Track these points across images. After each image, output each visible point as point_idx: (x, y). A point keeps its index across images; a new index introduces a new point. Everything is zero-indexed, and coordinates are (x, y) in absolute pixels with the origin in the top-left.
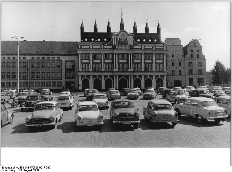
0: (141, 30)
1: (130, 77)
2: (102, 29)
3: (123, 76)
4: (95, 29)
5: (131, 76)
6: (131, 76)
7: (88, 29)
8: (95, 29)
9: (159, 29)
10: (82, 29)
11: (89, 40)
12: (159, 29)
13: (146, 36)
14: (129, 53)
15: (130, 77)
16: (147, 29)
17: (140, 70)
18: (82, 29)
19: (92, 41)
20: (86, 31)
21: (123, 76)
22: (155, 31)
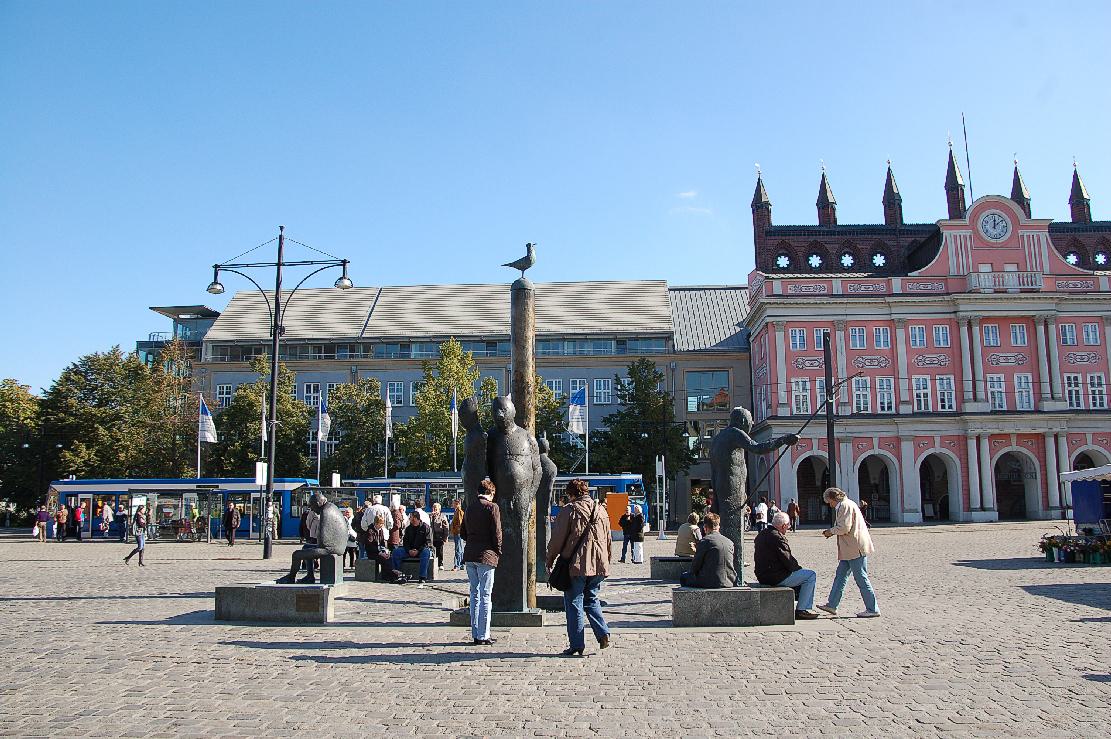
1: (1051, 442)
2: (860, 209)
3: (1014, 440)
4: (825, 206)
6: (1056, 437)
7: (795, 211)
8: (825, 206)
10: (760, 208)
11: (798, 266)
13: (1082, 237)
15: (1051, 442)
16: (1078, 201)
17: (1098, 407)
18: (760, 208)
19: (812, 270)
20: (777, 220)
21: (1014, 440)
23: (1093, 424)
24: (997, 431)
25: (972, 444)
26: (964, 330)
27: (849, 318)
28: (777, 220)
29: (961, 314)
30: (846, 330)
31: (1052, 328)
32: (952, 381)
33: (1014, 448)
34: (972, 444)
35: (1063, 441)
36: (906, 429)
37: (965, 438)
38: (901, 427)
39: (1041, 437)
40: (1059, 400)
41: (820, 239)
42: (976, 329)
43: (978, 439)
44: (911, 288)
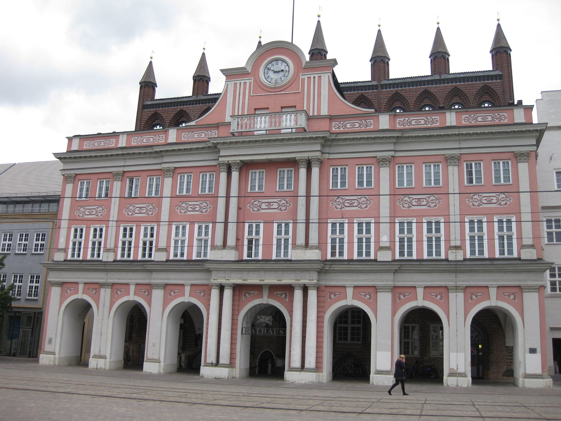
0: (410, 63)
1: (298, 294)
5: (305, 289)
6: (305, 289)
9: (501, 52)
10: (148, 85)
12: (501, 52)
14: (298, 156)
15: (298, 294)
20: (160, 94)
22: (484, 63)
23: (355, 277)
24: (240, 281)
26: (223, 176)
27: (126, 169)
28: (160, 94)
29: (221, 159)
31: (315, 171)
33: (265, 300)
34: (215, 293)
35: (313, 295)
36: (159, 278)
37: (208, 288)
38: (155, 275)
39: (290, 288)
40: (313, 248)
41: (185, 108)
42: (235, 175)
43: (222, 288)
44: (186, 137)
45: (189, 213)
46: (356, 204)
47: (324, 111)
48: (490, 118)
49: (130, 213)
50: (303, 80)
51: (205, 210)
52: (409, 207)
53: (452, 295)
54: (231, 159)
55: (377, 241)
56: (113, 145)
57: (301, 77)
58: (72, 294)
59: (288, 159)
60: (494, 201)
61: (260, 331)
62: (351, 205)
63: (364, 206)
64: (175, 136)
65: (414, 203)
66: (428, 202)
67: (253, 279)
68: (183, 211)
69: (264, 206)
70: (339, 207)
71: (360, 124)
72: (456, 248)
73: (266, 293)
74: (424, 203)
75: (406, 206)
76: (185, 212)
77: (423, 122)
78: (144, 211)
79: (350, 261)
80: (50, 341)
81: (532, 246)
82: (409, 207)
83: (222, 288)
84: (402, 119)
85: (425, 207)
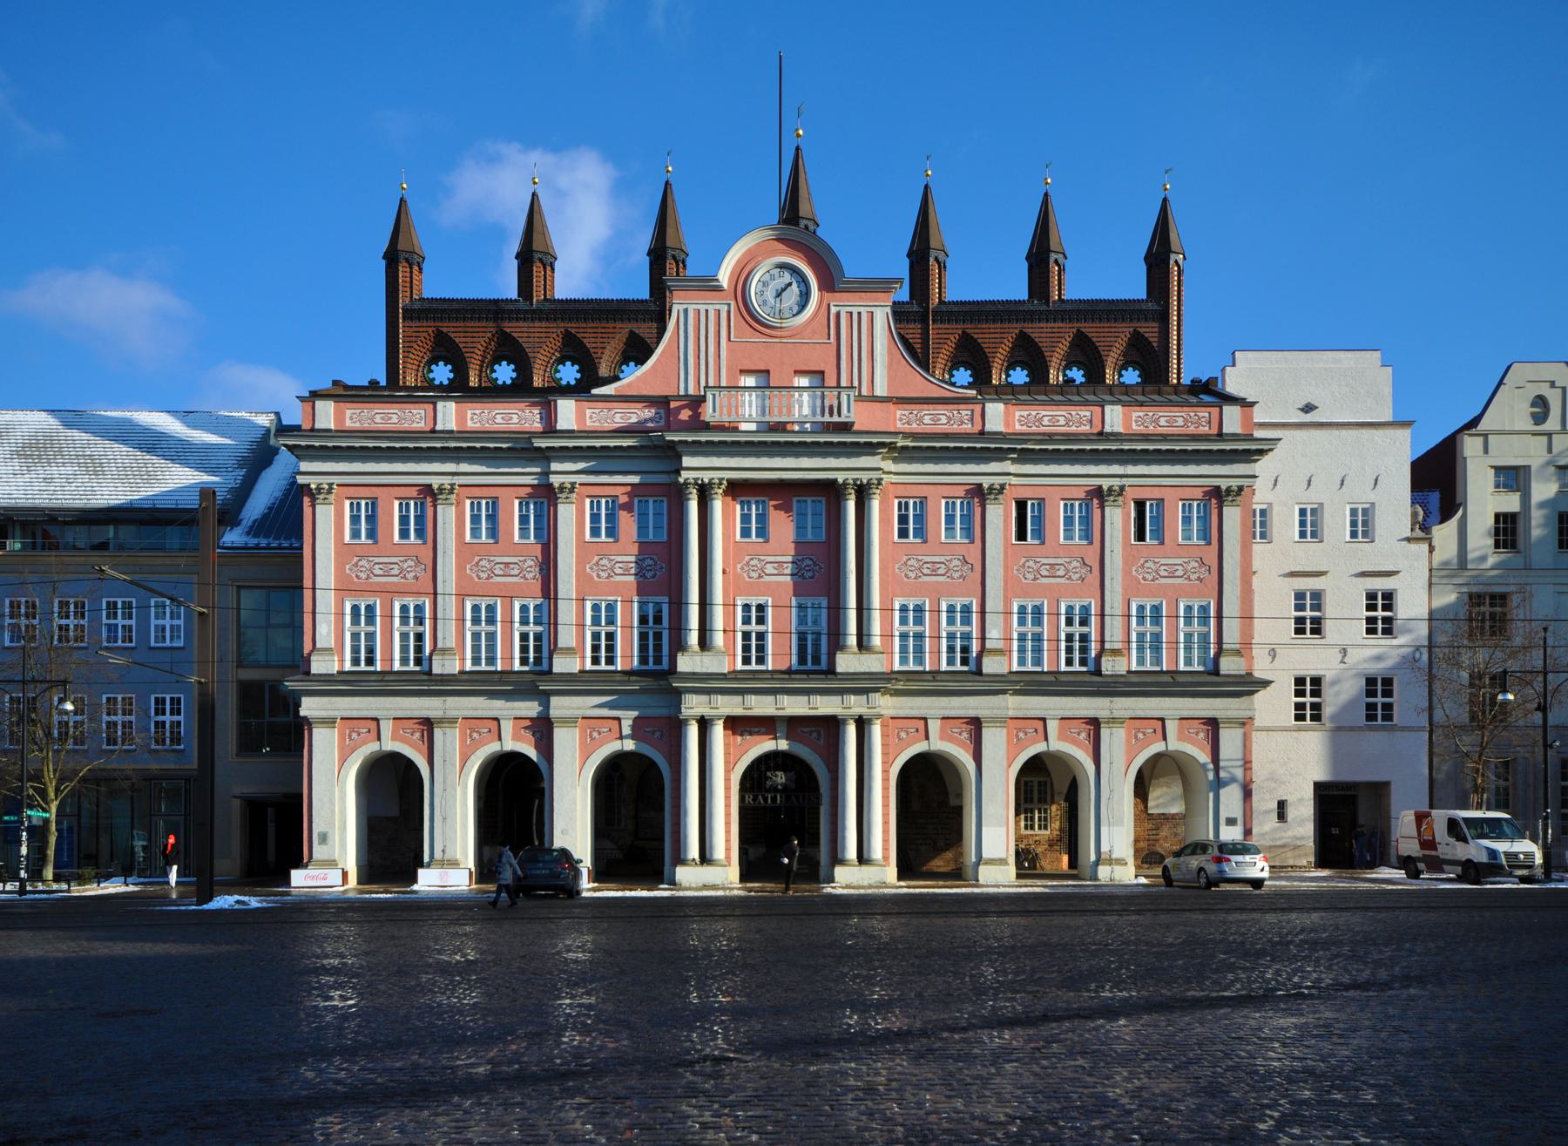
1: (851, 731)
5: (862, 724)
6: (862, 724)
14: (840, 477)
15: (851, 731)
24: (739, 711)
25: (693, 732)
30: (459, 504)
31: (875, 505)
32: (665, 609)
34: (693, 732)
35: (876, 731)
39: (832, 725)
42: (718, 506)
43: (704, 724)
45: (618, 578)
46: (941, 571)
47: (880, 390)
48: (1180, 422)
49: (484, 575)
50: (838, 315)
51: (649, 574)
52: (1035, 579)
53: (1105, 733)
54: (706, 477)
55: (983, 638)
56: (421, 425)
57: (833, 310)
58: (365, 743)
59: (818, 481)
60: (1180, 573)
61: (774, 799)
62: (934, 573)
63: (956, 575)
64: (573, 416)
65: (1044, 573)
66: (1068, 571)
67: (762, 706)
68: (604, 575)
69: (770, 569)
70: (912, 575)
71: (949, 419)
72: (1115, 652)
73: (782, 729)
74: (1061, 573)
75: (1030, 576)
76: (609, 576)
77: (1062, 422)
78: (516, 572)
79: (935, 673)
80: (324, 838)
81: (1238, 653)
82: (1035, 579)
83: (704, 724)
84: (1025, 413)
85: (1062, 580)
